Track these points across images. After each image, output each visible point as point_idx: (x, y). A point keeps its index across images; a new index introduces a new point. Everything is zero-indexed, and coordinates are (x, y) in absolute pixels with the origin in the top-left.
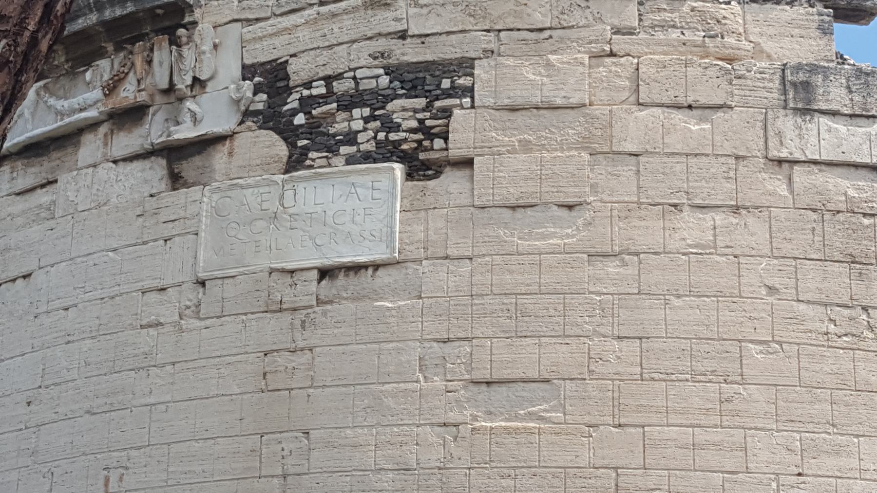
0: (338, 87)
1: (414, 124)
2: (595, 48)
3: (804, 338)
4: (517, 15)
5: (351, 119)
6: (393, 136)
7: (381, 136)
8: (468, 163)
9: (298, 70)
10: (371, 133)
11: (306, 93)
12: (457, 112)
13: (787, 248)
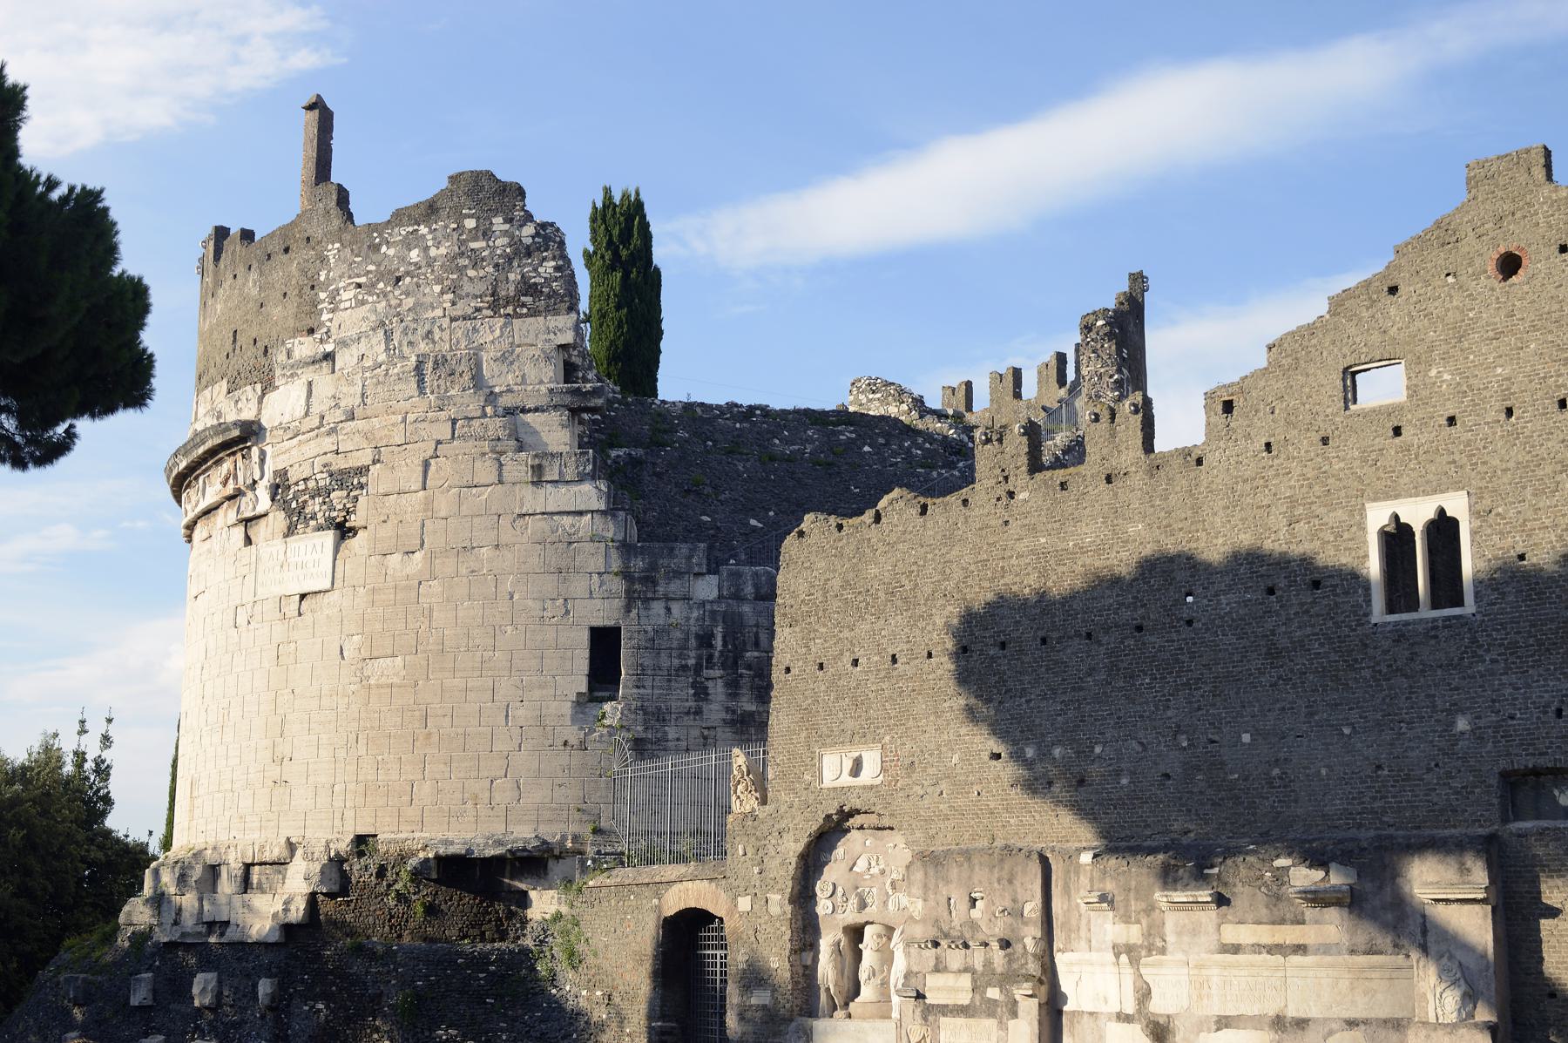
0: (311, 484)
6: (334, 514)
7: (327, 514)
9: (293, 476)
11: (296, 488)
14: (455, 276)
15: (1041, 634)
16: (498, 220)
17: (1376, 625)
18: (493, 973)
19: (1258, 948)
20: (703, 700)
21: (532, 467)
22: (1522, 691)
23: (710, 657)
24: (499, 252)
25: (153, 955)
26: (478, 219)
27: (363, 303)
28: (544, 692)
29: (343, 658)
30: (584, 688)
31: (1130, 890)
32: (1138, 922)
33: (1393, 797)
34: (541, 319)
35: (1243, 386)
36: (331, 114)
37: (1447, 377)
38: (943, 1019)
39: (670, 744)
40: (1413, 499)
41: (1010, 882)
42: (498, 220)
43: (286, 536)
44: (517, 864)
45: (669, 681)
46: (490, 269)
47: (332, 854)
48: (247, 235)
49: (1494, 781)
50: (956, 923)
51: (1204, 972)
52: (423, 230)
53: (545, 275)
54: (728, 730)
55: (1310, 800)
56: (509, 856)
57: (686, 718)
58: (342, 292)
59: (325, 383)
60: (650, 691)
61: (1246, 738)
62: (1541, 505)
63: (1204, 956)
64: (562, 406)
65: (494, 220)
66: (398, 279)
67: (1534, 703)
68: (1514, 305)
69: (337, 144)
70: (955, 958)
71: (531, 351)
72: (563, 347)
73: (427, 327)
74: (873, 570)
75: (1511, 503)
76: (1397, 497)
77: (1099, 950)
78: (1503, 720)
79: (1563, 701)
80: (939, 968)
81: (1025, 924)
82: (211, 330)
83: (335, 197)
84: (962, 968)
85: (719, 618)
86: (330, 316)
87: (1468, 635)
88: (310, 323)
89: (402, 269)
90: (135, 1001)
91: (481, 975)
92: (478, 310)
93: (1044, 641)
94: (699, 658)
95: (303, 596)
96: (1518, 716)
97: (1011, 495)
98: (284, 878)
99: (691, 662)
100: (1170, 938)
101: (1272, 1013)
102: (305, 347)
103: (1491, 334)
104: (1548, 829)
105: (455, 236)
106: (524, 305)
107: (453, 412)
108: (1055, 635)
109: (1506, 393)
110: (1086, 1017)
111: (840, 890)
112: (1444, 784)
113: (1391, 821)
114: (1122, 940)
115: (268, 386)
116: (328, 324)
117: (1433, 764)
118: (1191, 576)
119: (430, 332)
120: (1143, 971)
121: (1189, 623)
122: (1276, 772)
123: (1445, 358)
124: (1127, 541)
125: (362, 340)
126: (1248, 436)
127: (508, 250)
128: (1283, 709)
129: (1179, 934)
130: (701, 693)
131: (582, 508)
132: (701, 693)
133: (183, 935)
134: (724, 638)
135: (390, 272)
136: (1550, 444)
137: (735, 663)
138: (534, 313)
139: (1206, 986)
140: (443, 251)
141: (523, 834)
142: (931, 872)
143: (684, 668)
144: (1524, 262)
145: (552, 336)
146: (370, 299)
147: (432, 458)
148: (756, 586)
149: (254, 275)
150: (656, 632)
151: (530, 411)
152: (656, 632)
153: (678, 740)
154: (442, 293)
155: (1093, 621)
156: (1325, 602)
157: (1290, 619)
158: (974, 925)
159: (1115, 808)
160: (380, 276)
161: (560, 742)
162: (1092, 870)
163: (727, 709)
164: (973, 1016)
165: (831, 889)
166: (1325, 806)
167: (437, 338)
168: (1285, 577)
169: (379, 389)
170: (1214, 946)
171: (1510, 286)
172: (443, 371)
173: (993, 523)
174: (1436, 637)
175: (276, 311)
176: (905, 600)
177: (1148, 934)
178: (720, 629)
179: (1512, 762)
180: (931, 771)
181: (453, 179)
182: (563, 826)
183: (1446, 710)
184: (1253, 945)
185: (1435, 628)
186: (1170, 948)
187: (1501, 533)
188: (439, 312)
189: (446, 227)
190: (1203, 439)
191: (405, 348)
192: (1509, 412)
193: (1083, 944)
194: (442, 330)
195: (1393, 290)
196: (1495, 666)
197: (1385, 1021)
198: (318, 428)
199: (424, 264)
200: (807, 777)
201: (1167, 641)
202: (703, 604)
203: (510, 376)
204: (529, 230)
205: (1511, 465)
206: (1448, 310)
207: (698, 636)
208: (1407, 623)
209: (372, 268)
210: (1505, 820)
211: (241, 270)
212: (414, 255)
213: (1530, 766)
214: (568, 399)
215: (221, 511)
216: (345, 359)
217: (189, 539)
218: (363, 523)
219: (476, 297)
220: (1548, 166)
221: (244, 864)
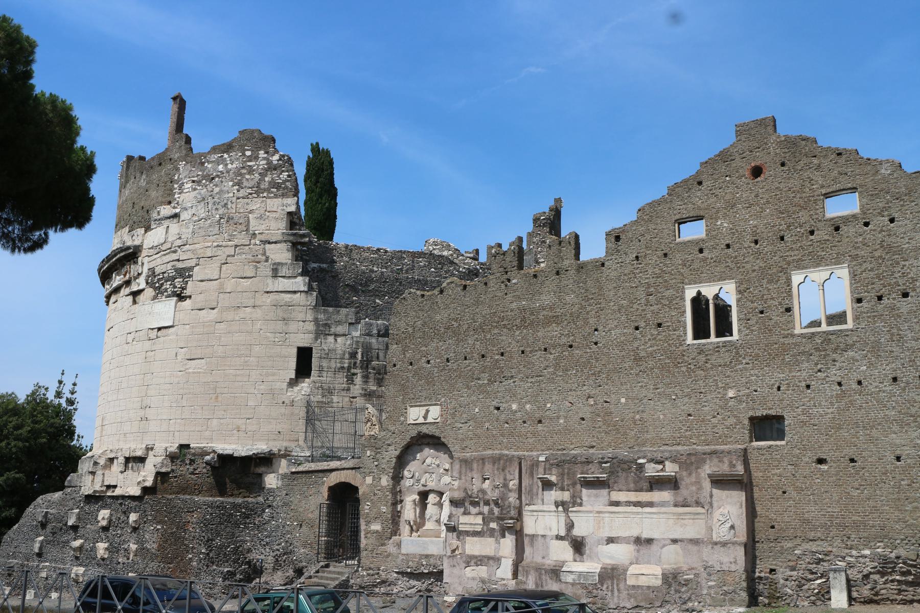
0: (166, 275)
1: (179, 286)
2: (223, 262)
3: (268, 343)
4: (205, 253)
5: (166, 285)
6: (175, 290)
8: (190, 297)
9: (158, 270)
10: (170, 289)
12: (189, 282)
13: (267, 318)
14: (239, 178)
15: (522, 349)
16: (262, 152)
17: (689, 345)
18: (244, 513)
19: (629, 504)
20: (350, 384)
21: (272, 269)
22: (761, 378)
23: (355, 363)
24: (261, 167)
25: (80, 501)
26: (252, 151)
27: (195, 189)
28: (274, 378)
29: (177, 359)
30: (293, 376)
31: (564, 475)
32: (568, 490)
33: (696, 430)
34: (280, 199)
35: (624, 229)
36: (185, 102)
37: (725, 225)
38: (467, 538)
39: (334, 404)
40: (708, 284)
41: (503, 470)
42: (262, 152)
43: (153, 300)
44: (258, 460)
45: (335, 374)
46: (257, 175)
47: (168, 453)
48: (142, 158)
49: (746, 422)
50: (475, 491)
51: (601, 515)
52: (226, 156)
53: (282, 179)
54: (362, 398)
55: (654, 431)
56: (254, 456)
57: (342, 392)
58: (185, 184)
59: (174, 227)
60: (325, 379)
61: (623, 400)
62: (771, 287)
63: (602, 507)
64: (289, 241)
65: (260, 152)
66: (213, 179)
67: (767, 384)
68: (758, 191)
69: (186, 116)
70: (474, 510)
71: (274, 215)
72: (290, 214)
73: (225, 202)
74: (438, 317)
75: (757, 287)
76: (700, 283)
77: (548, 504)
78: (751, 392)
79: (781, 384)
80: (466, 513)
81: (510, 491)
82: (123, 203)
83: (184, 140)
84: (477, 512)
85: (360, 345)
86: (179, 195)
87: (734, 350)
88: (169, 199)
89: (214, 174)
90: (70, 523)
91: (238, 514)
92: (251, 194)
93: (523, 352)
94: (350, 363)
95: (159, 329)
96: (759, 390)
97: (509, 280)
98: (144, 466)
99: (346, 365)
100: (584, 498)
101: (635, 536)
102: (166, 210)
103: (747, 205)
104: (772, 445)
105: (241, 159)
106: (272, 192)
107: (236, 242)
108: (529, 349)
109: (755, 233)
110: (540, 537)
111: (417, 474)
112: (722, 423)
113: (695, 442)
114: (560, 499)
115: (148, 229)
116: (178, 199)
117: (716, 414)
118: (597, 321)
119: (226, 204)
120: (570, 514)
121: (596, 344)
122: (638, 417)
123: (725, 216)
124: (565, 304)
125: (194, 207)
126: (626, 254)
127: (266, 166)
128: (641, 386)
129: (589, 496)
130: (350, 379)
131: (296, 289)
132: (350, 379)
133: (95, 491)
134: (362, 354)
135: (209, 176)
136: (775, 258)
137: (367, 367)
138: (276, 196)
139: (602, 522)
140: (234, 166)
141: (261, 447)
142: (464, 466)
143: (343, 368)
144: (764, 170)
145: (285, 208)
146: (199, 188)
147: (224, 264)
148: (379, 331)
149: (144, 177)
150: (329, 350)
151: (272, 243)
152: (329, 350)
153: (338, 402)
154: (233, 186)
155: (548, 342)
156: (664, 334)
157: (646, 343)
158: (483, 492)
160: (204, 177)
161: (281, 402)
162: (545, 465)
163: (363, 389)
164: (482, 537)
165: (412, 473)
166: (662, 434)
167: (229, 207)
168: (644, 322)
169: (200, 231)
170: (607, 502)
171: (757, 182)
172: (231, 222)
173: (499, 294)
174: (719, 351)
175: (153, 194)
176: (454, 332)
177: (573, 497)
178: (360, 350)
179: (755, 413)
180: (465, 416)
181: (241, 132)
182: (281, 442)
183: (723, 387)
184: (626, 502)
186: (584, 503)
187: (752, 302)
188: (231, 195)
189: (237, 155)
190: (605, 254)
191: (213, 211)
192: (756, 242)
193: (540, 501)
194: (232, 203)
195: (700, 183)
196: (747, 366)
197: (691, 540)
198: (170, 249)
199: (225, 172)
200: (402, 419)
201: (585, 353)
202: (353, 338)
203: (263, 226)
204: (276, 157)
205: (756, 268)
206: (726, 193)
207: (349, 353)
208: (704, 345)
209: (200, 173)
210: (751, 441)
211: (138, 175)
212: (221, 168)
213: (764, 414)
214: (291, 238)
215: (122, 290)
216: (185, 216)
217: (108, 303)
218: (190, 294)
219: (250, 188)
220: (775, 126)
221: (125, 457)
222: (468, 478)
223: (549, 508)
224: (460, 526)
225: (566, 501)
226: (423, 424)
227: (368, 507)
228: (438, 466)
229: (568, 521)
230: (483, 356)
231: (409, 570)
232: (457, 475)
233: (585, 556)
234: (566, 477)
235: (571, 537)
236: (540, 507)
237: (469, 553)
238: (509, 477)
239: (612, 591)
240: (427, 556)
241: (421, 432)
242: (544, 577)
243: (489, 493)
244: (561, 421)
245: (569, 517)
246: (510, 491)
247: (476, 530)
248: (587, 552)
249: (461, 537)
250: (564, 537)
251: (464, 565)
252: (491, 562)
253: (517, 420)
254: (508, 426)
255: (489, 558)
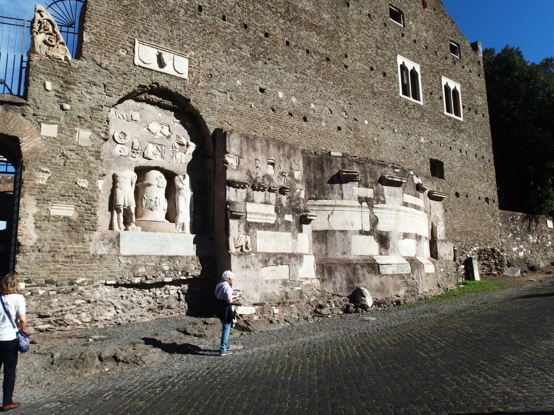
32: (372, 188)
38: (260, 233)
41: (289, 158)
50: (260, 175)
61: (366, 122)
100: (387, 197)
110: (337, 234)
120: (374, 210)
159: (320, 135)
164: (277, 230)
170: (402, 203)
177: (376, 194)
180: (224, 84)
185: (414, 105)
186: (387, 201)
193: (336, 195)
200: (123, 53)
222: (251, 159)
223: (351, 203)
224: (248, 216)
225: (370, 198)
226: (161, 73)
227: (46, 176)
228: (168, 137)
229: (372, 216)
230: (245, 26)
231: (137, 280)
232: (238, 153)
233: (389, 250)
234: (368, 174)
235: (377, 232)
236: (339, 202)
237: (262, 251)
238: (294, 166)
239: (419, 279)
240: (171, 258)
241: (157, 84)
242: (360, 272)
243: (275, 181)
244: (323, 124)
245: (373, 213)
246: (297, 181)
247: (269, 222)
248: (391, 246)
249: (251, 231)
250: (370, 232)
251: (261, 265)
252: (293, 259)
253: (283, 109)
254: (273, 112)
255: (291, 255)
